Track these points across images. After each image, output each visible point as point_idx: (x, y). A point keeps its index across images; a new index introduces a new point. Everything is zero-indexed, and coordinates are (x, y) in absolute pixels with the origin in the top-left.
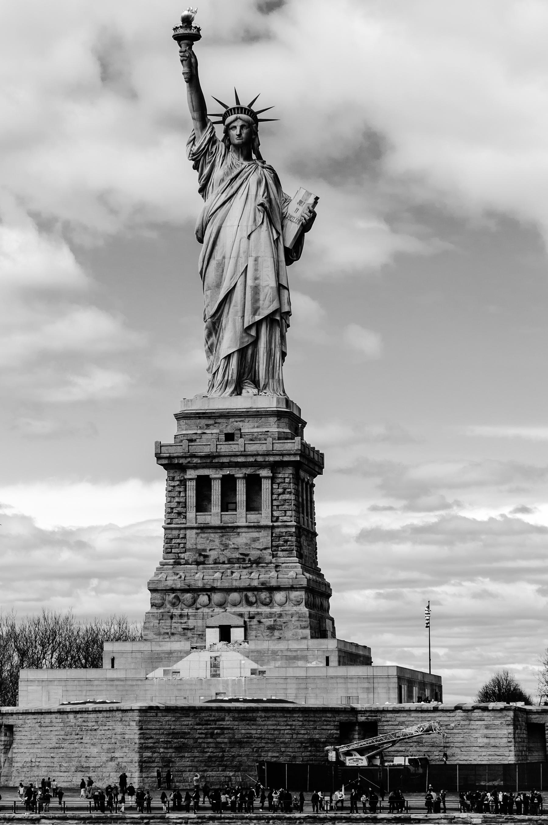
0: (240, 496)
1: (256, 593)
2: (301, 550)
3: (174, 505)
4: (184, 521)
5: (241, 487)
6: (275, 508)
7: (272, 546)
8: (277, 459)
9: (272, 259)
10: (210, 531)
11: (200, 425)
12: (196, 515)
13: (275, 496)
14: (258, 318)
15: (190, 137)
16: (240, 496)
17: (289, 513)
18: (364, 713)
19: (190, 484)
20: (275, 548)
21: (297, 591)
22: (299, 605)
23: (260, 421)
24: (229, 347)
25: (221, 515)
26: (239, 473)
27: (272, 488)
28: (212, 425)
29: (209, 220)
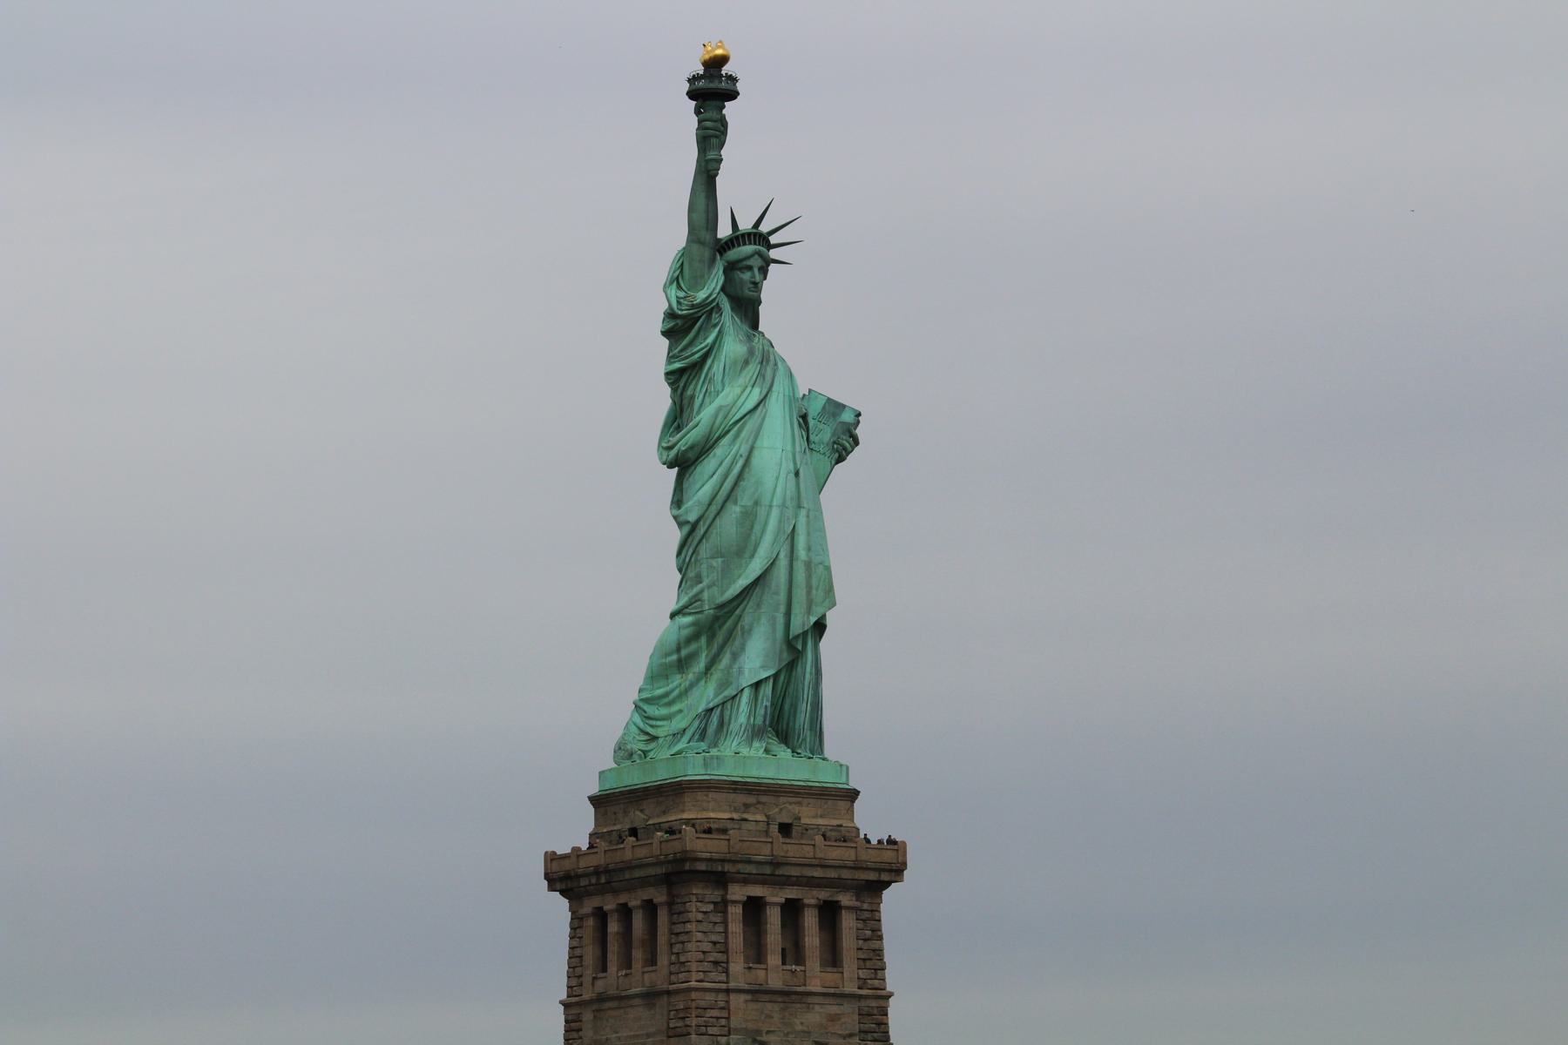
0: (811, 938)
3: (707, 947)
4: (723, 977)
5: (810, 920)
6: (861, 962)
8: (872, 876)
10: (767, 997)
11: (735, 805)
14: (813, 619)
15: (674, 272)
16: (811, 938)
19: (734, 912)
20: (862, 1035)
23: (826, 806)
24: (764, 667)
28: (754, 805)
29: (728, 432)
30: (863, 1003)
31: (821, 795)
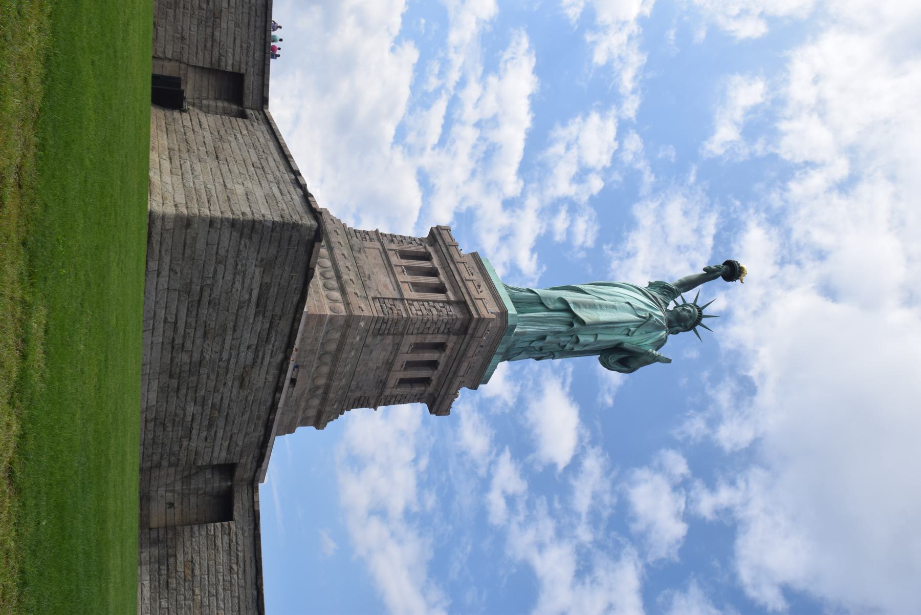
1: (335, 278)
2: (380, 334)
5: (432, 280)
7: (384, 298)
8: (469, 302)
9: (617, 320)
10: (384, 257)
12: (394, 250)
13: (431, 303)
17: (419, 313)
18: (260, 114)
21: (346, 309)
22: (331, 310)
25: (401, 266)
26: (443, 277)
27: (439, 302)
30: (398, 303)
31: (496, 298)
